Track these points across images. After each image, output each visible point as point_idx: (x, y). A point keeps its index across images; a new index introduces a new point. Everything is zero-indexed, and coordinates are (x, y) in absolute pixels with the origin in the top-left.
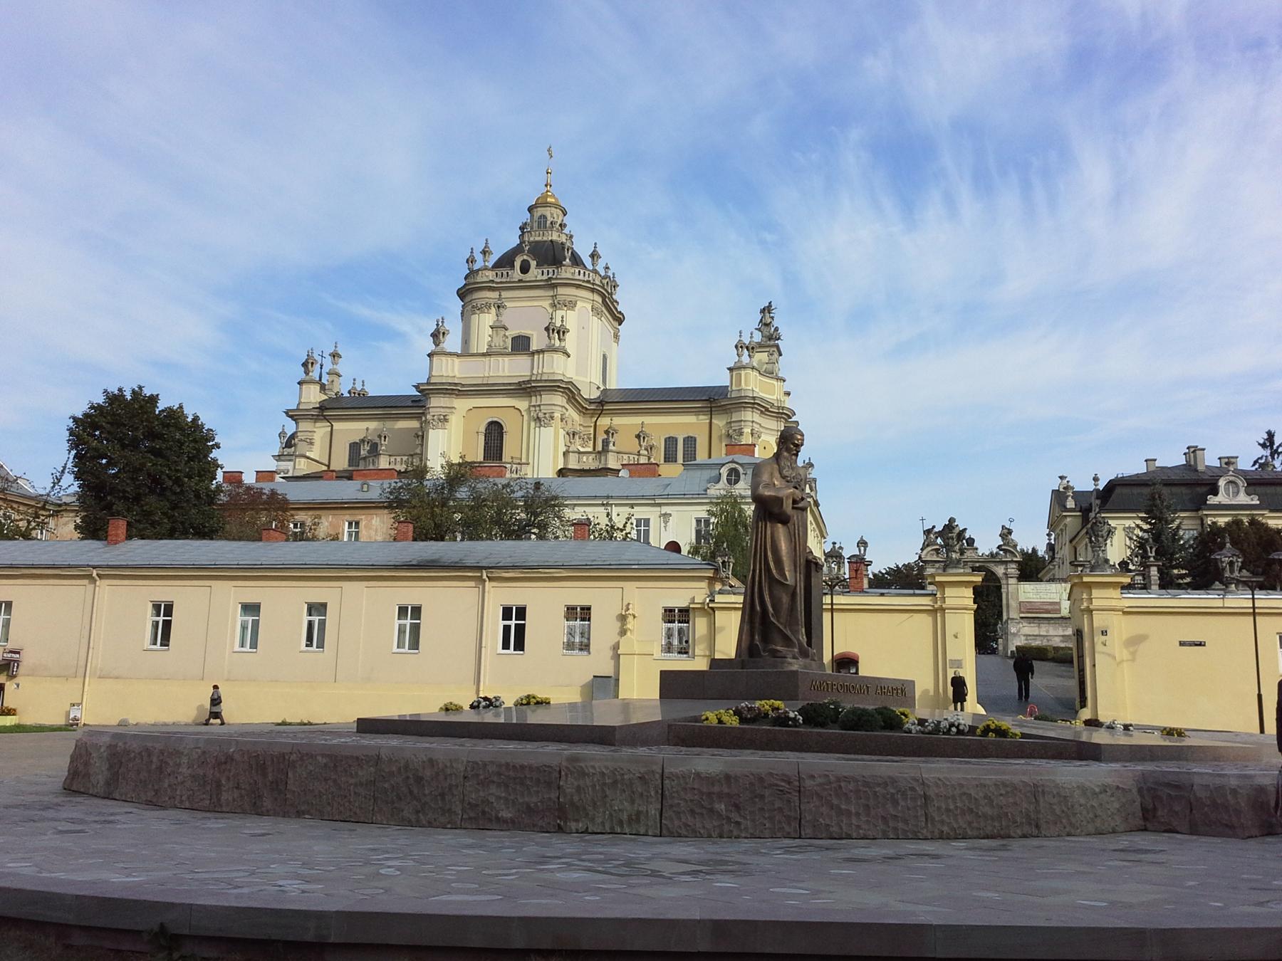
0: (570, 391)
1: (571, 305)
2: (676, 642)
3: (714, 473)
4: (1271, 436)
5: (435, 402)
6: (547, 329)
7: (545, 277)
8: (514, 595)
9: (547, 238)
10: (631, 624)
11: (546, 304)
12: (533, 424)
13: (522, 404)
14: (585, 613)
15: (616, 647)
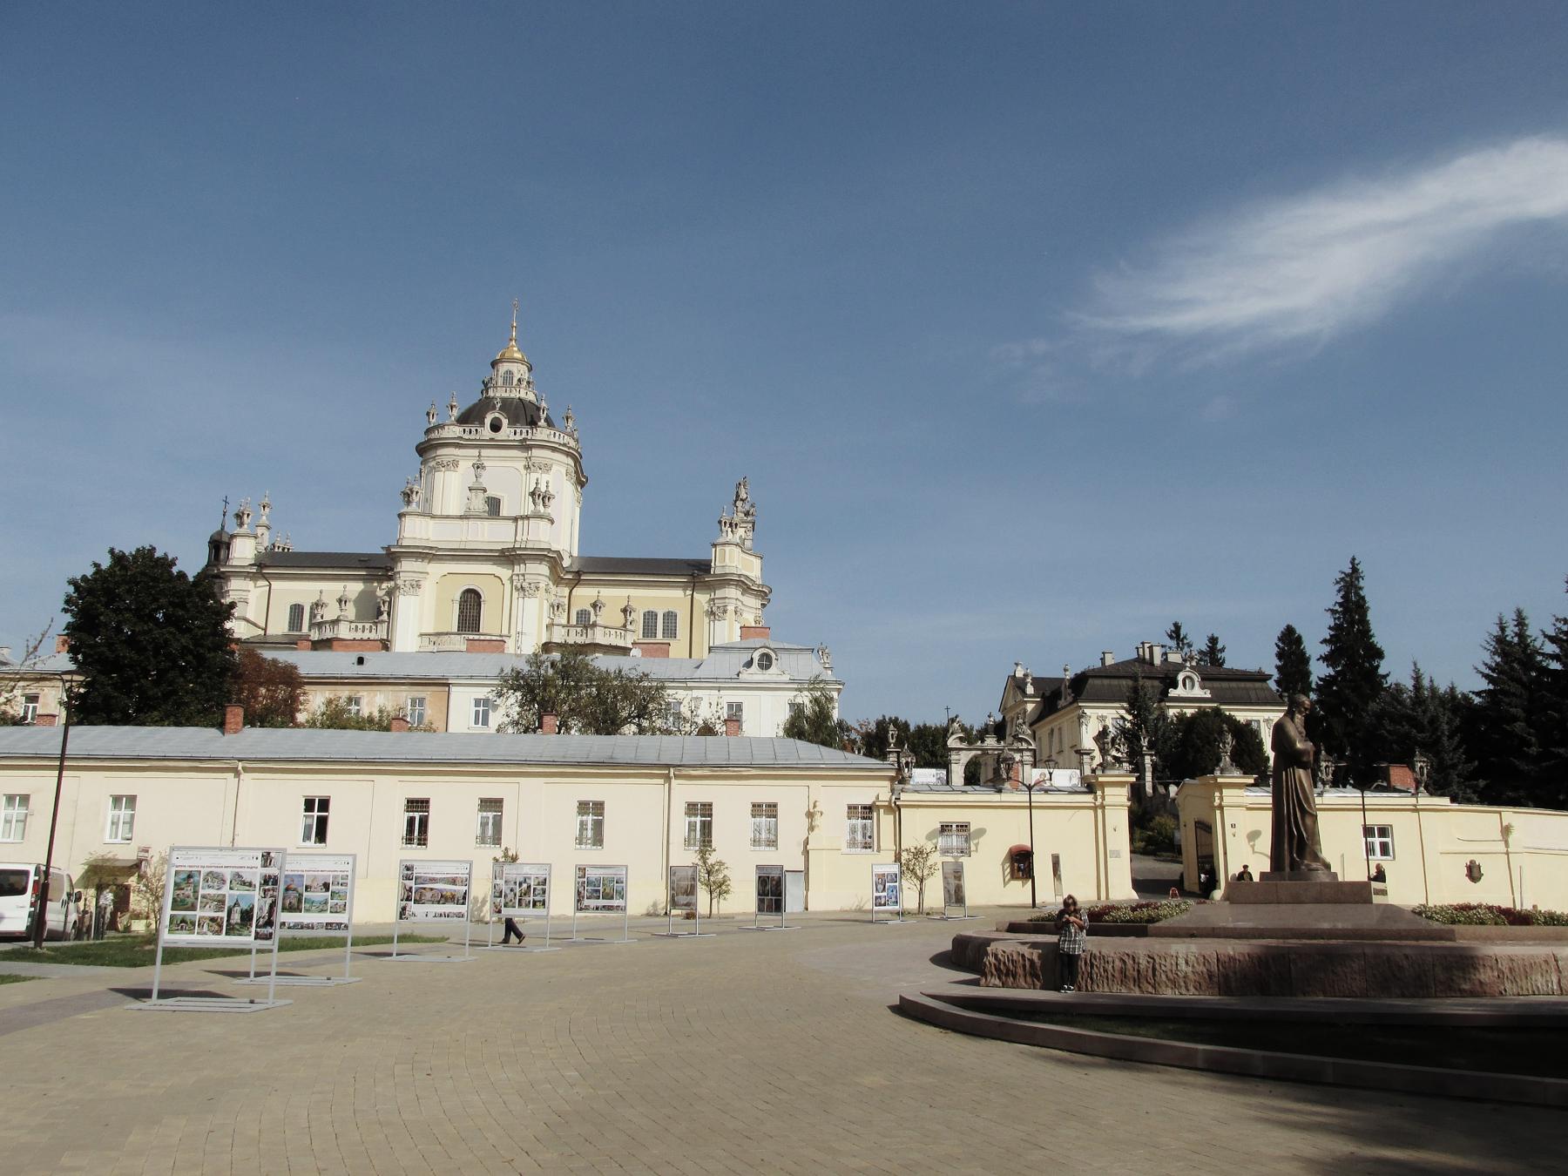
0: (552, 559)
1: (546, 468)
2: (859, 837)
3: (746, 658)
4: (1177, 627)
5: (406, 567)
6: (533, 494)
7: (518, 437)
8: (700, 791)
9: (514, 394)
10: (818, 820)
11: (521, 465)
12: (515, 594)
13: (504, 572)
14: (771, 810)
15: (806, 843)
